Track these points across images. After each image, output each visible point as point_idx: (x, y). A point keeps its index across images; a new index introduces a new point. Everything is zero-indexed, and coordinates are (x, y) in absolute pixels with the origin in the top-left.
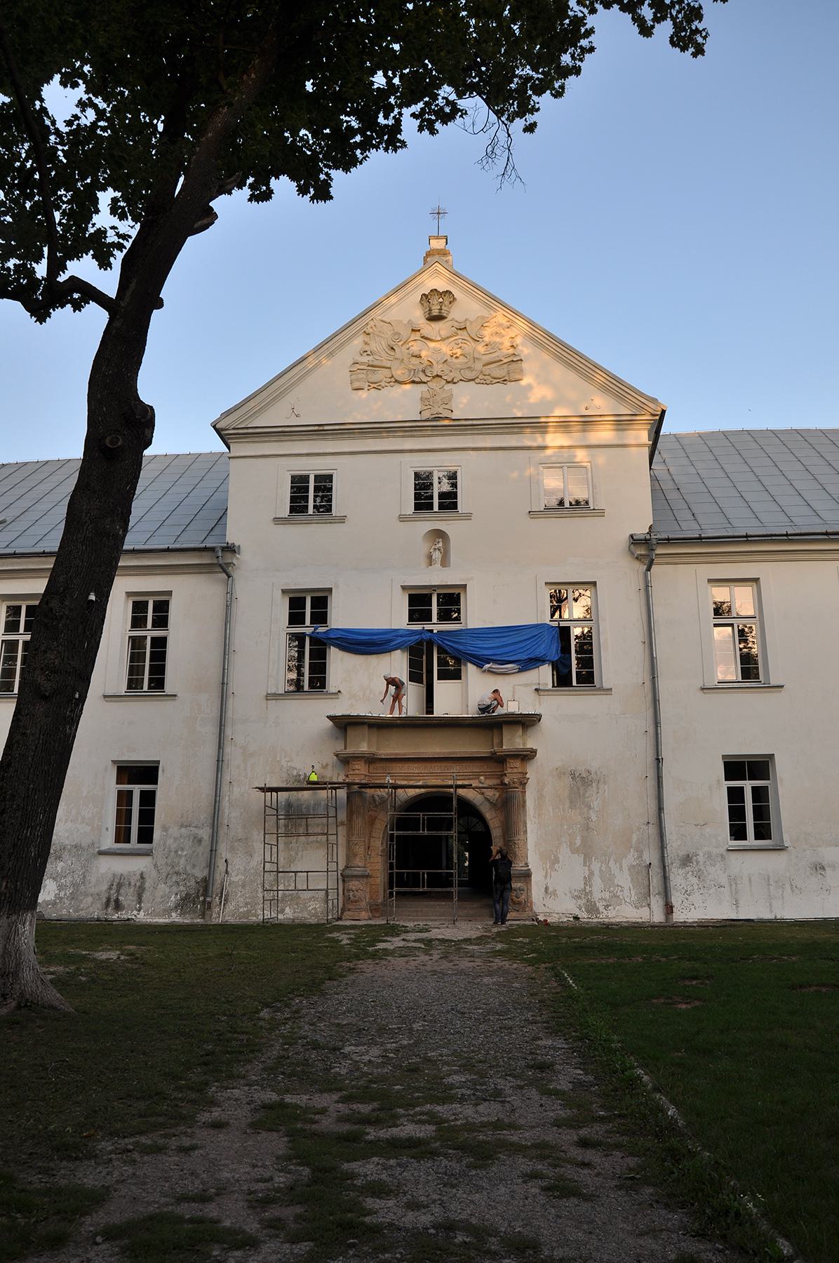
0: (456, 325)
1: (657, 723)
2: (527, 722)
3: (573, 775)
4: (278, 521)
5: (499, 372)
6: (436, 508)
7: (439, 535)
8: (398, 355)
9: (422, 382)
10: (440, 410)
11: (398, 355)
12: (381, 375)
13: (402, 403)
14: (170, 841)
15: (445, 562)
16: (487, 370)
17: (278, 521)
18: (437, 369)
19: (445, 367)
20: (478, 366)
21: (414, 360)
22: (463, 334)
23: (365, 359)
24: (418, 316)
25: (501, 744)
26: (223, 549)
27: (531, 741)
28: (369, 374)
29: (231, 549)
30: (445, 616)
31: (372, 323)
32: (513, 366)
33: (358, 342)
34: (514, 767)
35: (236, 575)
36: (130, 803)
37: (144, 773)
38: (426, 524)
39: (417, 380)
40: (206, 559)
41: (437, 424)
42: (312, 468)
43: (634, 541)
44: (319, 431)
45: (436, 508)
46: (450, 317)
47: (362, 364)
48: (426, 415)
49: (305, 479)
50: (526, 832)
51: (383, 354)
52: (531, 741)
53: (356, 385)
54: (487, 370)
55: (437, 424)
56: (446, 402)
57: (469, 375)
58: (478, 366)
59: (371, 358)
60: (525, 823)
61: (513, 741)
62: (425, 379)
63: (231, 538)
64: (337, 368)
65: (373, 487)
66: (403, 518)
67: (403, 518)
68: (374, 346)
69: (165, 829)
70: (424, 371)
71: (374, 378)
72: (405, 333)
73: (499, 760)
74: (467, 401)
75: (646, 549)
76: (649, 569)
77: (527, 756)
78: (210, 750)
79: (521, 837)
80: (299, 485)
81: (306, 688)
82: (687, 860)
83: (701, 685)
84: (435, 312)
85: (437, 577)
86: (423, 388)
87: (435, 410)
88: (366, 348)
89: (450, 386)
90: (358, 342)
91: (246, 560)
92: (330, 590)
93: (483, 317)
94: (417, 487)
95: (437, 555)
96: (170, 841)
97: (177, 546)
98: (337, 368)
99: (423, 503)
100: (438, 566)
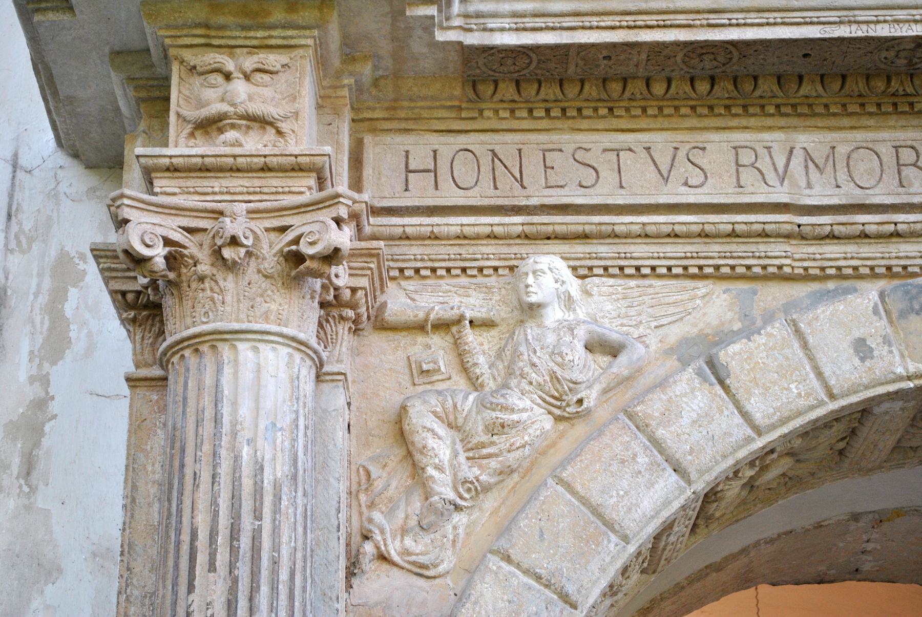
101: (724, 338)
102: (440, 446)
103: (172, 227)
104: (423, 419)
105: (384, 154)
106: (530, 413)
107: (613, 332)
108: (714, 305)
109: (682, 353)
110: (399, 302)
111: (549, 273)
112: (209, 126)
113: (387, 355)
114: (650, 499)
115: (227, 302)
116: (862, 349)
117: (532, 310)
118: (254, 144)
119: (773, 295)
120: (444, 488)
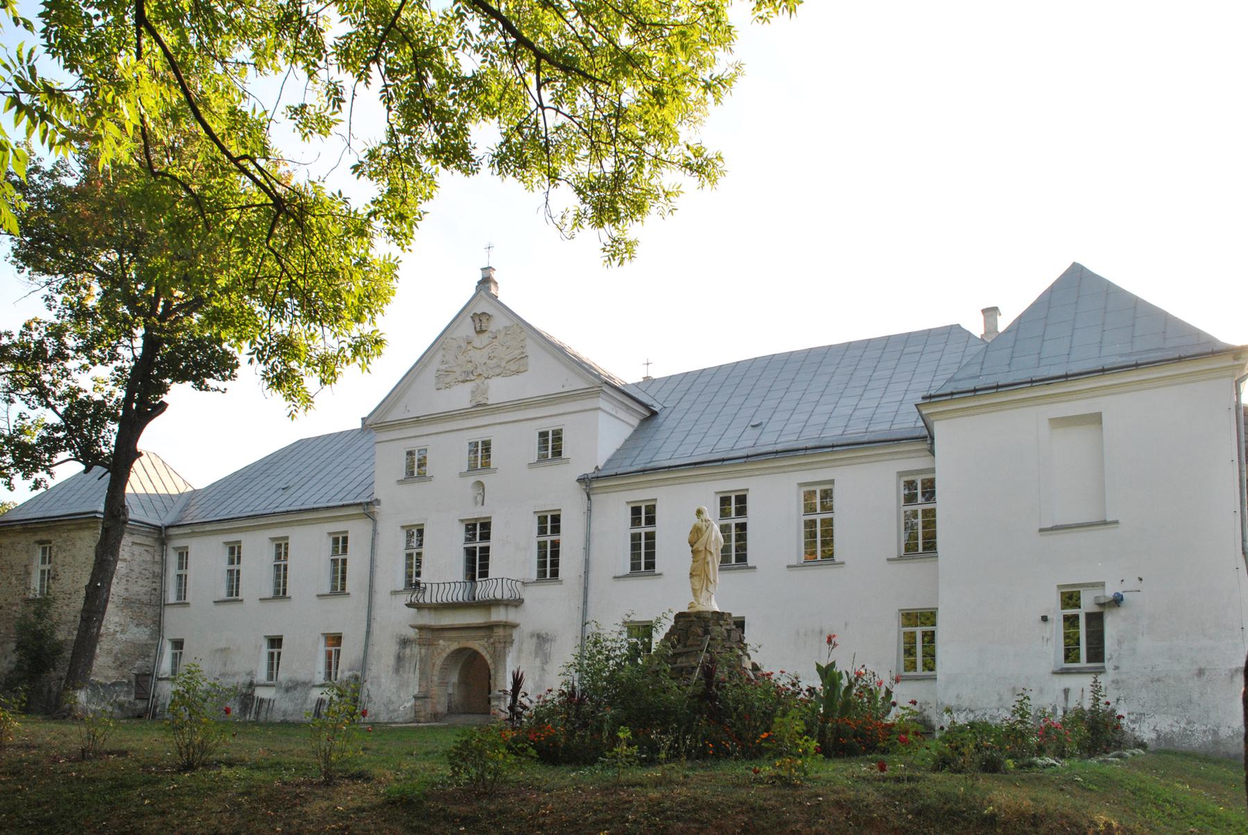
1: (585, 602)
5: (513, 367)
7: (480, 484)
13: (460, 397)
17: (400, 482)
18: (479, 371)
20: (503, 364)
23: (443, 367)
24: (472, 333)
28: (444, 379)
32: (522, 361)
37: (335, 640)
38: (472, 479)
44: (418, 421)
48: (474, 403)
55: (481, 408)
56: (485, 392)
57: (498, 371)
65: (448, 453)
67: (462, 475)
74: (500, 390)
79: (500, 674)
90: (439, 357)
95: (479, 498)
114: (445, 655)
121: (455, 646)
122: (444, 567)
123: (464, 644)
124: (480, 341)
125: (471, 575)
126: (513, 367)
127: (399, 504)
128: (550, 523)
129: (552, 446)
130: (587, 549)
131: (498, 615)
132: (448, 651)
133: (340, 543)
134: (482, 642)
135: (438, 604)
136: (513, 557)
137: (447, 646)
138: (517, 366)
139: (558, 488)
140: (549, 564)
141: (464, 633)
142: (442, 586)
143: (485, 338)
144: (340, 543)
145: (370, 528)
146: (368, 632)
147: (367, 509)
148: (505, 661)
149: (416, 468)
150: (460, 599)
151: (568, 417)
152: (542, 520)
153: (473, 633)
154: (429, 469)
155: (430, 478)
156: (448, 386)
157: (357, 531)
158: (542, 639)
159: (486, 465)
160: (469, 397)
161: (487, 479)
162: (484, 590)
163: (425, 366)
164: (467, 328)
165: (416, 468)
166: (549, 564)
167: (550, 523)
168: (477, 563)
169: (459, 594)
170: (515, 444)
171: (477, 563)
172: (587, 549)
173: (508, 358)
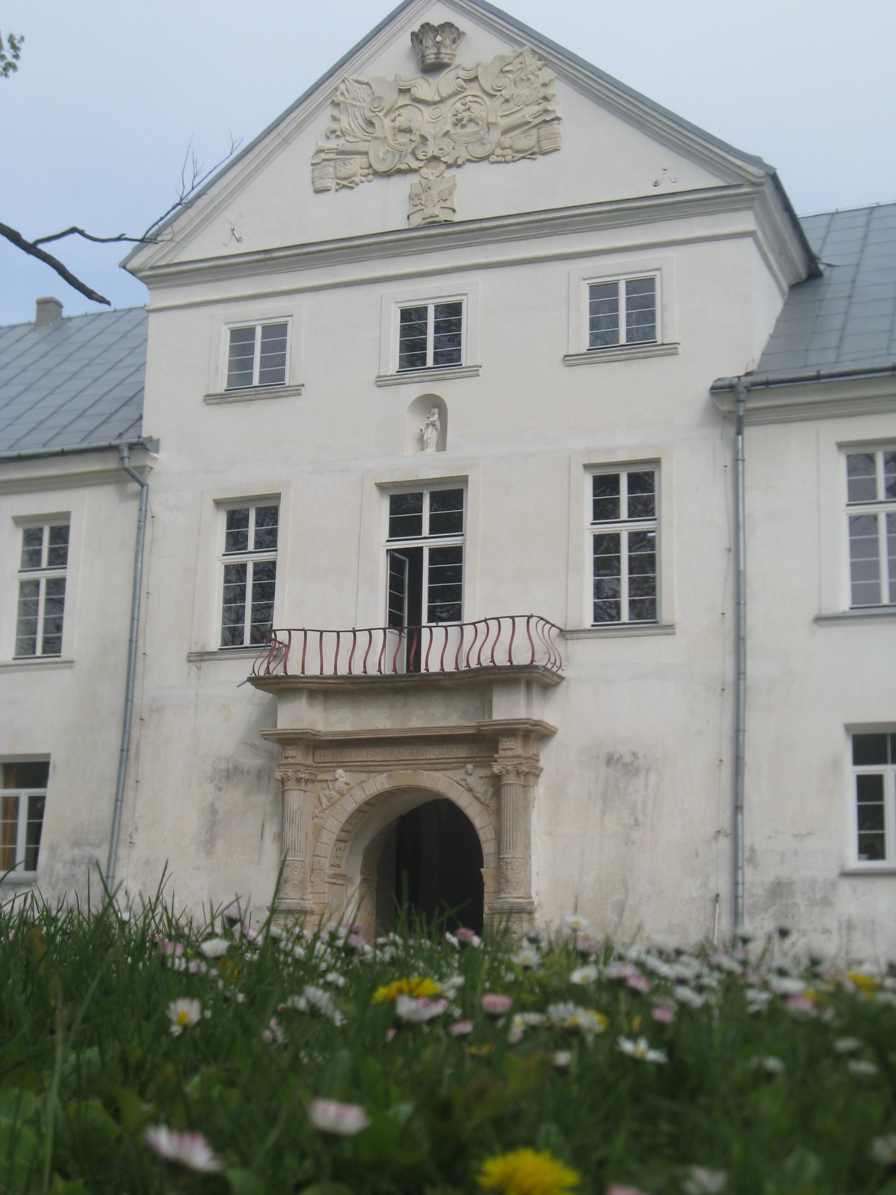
0: (463, 74)
2: (535, 679)
3: (610, 760)
4: (570, 360)
5: (522, 141)
6: (430, 362)
7: (432, 405)
8: (378, 133)
9: (411, 171)
10: (437, 211)
11: (378, 133)
12: (356, 164)
13: (382, 207)
14: (58, 866)
15: (442, 445)
16: (506, 141)
17: (212, 399)
18: (432, 149)
19: (446, 143)
21: (403, 139)
22: (473, 89)
23: (332, 144)
24: (408, 71)
25: (490, 716)
26: (132, 447)
27: (544, 711)
28: (336, 170)
29: (142, 446)
30: (437, 527)
31: (342, 87)
32: (546, 129)
33: (323, 121)
34: (511, 748)
35: (152, 481)
36: (15, 815)
38: (414, 390)
39: (403, 167)
40: (110, 463)
41: (438, 233)
42: (257, 314)
43: (723, 390)
45: (430, 362)
46: (456, 62)
47: (330, 151)
48: (416, 220)
49: (421, 312)
50: (527, 847)
51: (360, 133)
52: (544, 711)
53: (320, 184)
54: (506, 141)
55: (438, 233)
57: (480, 152)
58: (495, 136)
59: (341, 141)
60: (527, 834)
61: (508, 708)
62: (415, 165)
63: (148, 430)
64: (295, 161)
65: (344, 336)
66: (382, 382)
67: (382, 382)
68: (344, 124)
69: (53, 849)
70: (413, 153)
71: (344, 171)
72: (390, 97)
73: (484, 742)
74: (481, 192)
75: (736, 403)
76: (739, 432)
77: (536, 734)
78: (112, 736)
80: (412, 319)
81: (247, 641)
82: (779, 890)
83: (813, 613)
84: (431, 59)
85: (427, 467)
86: (413, 179)
87: (428, 212)
88: (335, 126)
89: (449, 173)
90: (323, 121)
91: (165, 463)
92: (657, 462)
93: (502, 58)
94: (405, 331)
95: (431, 435)
96: (58, 866)
97: (14, 453)
98: (295, 161)
99: (412, 354)
100: (431, 449)
101: (363, 782)
102: (324, 800)
103: (281, 774)
104: (322, 796)
105: (318, 754)
106: (337, 796)
107: (348, 781)
108: (363, 776)
109: (359, 784)
110: (320, 777)
111: (340, 772)
112: (286, 758)
113: (318, 785)
114: (350, 806)
115: (290, 785)
116: (382, 784)
117: (336, 780)
118: (291, 760)
119: (373, 774)
120: (324, 807)
121: (378, 783)
122: (335, 599)
123: (404, 778)
124: (425, 89)
125: (403, 615)
126: (522, 141)
127: (203, 449)
128: (625, 489)
129: (624, 322)
130: (736, 550)
131: (508, 708)
132: (360, 796)
133: (48, 542)
134: (459, 775)
135: (350, 678)
136: (524, 573)
137: (356, 786)
138: (534, 139)
139: (648, 409)
140: (627, 584)
141: (406, 754)
142: (347, 638)
143: (445, 82)
144: (48, 542)
145: (133, 507)
146: (124, 751)
147: (124, 459)
148: (527, 821)
149: (258, 365)
150: (372, 671)
151: (673, 253)
152: (605, 485)
153: (433, 753)
154: (296, 368)
155: (297, 391)
156: (346, 184)
157: (93, 514)
158: (620, 766)
159: (449, 355)
160: (406, 209)
161: (449, 390)
162: (439, 649)
163: (286, 141)
164: (395, 60)
165: (258, 365)
166: (627, 584)
167: (625, 489)
168: (426, 585)
169: (379, 655)
170: (521, 316)
171: (426, 585)
172: (736, 550)
173: (505, 123)
